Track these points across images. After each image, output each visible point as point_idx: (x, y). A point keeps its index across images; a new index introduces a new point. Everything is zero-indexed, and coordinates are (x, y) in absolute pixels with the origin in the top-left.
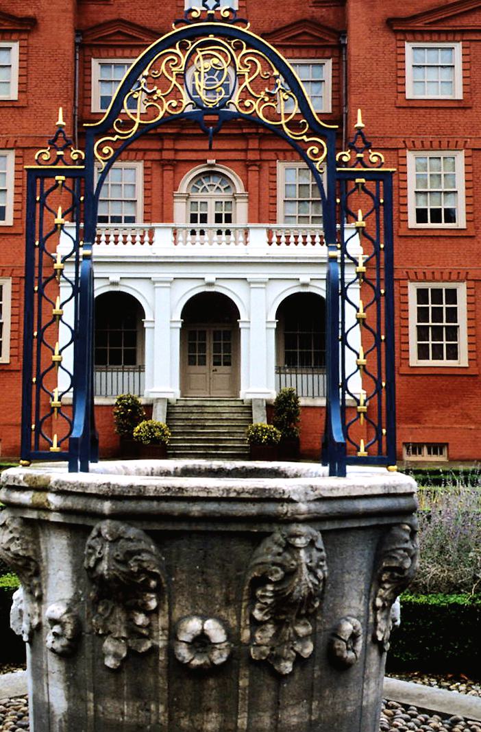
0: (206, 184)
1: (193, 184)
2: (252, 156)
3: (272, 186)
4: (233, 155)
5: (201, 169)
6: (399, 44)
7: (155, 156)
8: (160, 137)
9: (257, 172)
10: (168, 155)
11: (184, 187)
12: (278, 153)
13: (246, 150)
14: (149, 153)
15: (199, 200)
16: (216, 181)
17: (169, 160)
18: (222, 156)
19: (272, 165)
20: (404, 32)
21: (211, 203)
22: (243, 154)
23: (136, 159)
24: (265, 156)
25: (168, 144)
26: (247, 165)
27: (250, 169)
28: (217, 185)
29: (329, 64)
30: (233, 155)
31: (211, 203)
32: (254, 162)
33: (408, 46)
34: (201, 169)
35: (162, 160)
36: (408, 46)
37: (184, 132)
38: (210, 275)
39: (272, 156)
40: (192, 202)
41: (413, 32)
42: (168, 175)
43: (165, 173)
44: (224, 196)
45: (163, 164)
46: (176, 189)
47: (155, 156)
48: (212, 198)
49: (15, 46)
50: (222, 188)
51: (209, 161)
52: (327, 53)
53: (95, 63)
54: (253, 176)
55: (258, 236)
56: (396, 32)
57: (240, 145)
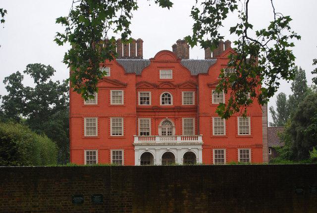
4: (172, 116)
5: (164, 120)
8: (155, 112)
10: (156, 117)
11: (160, 125)
21: (167, 128)
25: (157, 114)
26: (175, 119)
29: (194, 93)
30: (172, 116)
31: (167, 128)
32: (177, 118)
34: (164, 120)
39: (181, 116)
44: (170, 126)
48: (167, 127)
49: (123, 91)
55: (179, 139)
57: (173, 114)
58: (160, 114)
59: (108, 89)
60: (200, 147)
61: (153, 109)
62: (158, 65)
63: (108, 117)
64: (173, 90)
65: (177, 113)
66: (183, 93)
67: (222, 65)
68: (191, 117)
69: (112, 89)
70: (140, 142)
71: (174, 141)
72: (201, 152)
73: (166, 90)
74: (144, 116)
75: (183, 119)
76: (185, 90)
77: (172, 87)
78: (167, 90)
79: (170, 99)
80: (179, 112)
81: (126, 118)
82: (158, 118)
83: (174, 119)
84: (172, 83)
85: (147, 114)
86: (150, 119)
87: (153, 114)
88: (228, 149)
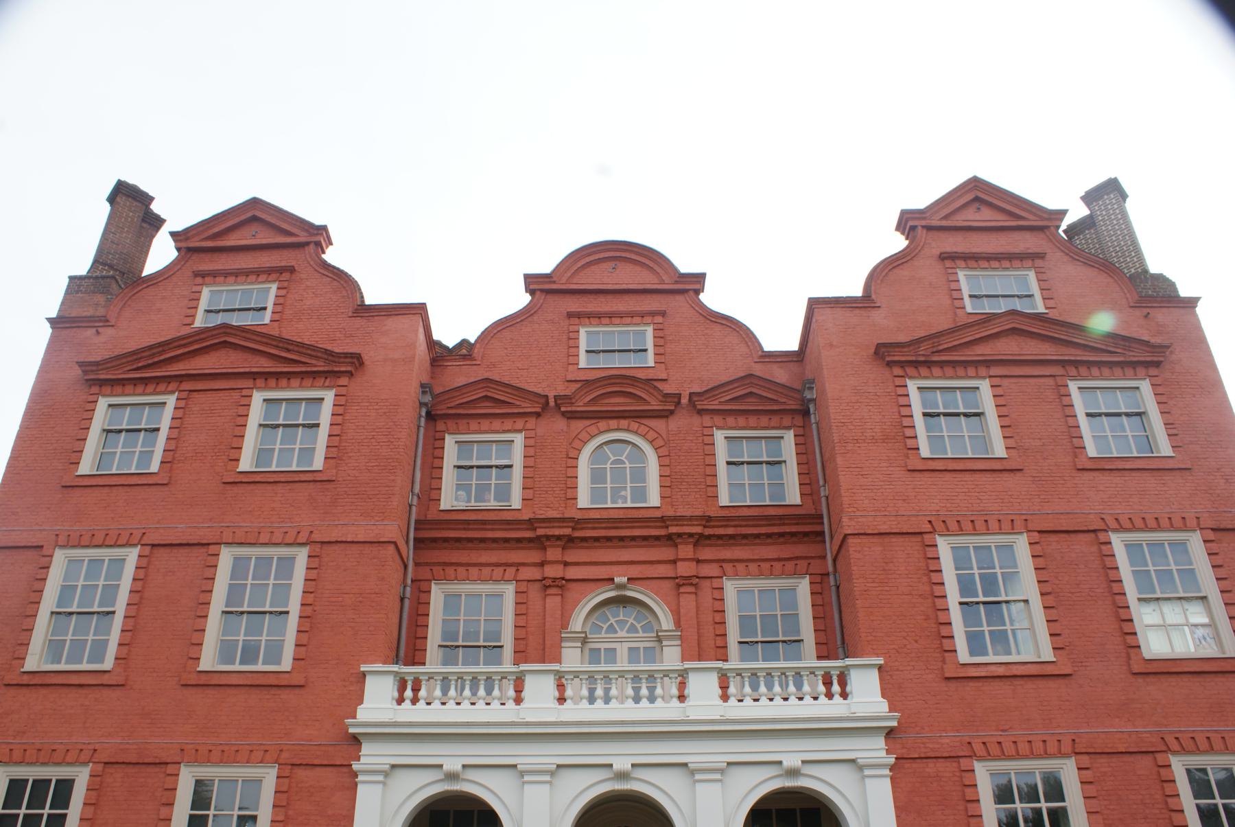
0: (612, 621)
1: (593, 619)
2: (684, 569)
3: (717, 605)
6: (898, 381)
7: (533, 573)
9: (694, 596)
10: (552, 571)
11: (577, 623)
12: (724, 565)
13: (674, 562)
14: (522, 569)
15: (603, 646)
16: (628, 616)
17: (554, 579)
18: (635, 571)
19: (716, 583)
20: (902, 364)
22: (669, 567)
23: (503, 580)
24: (706, 570)
25: (553, 553)
27: (682, 590)
28: (631, 620)
29: (789, 437)
33: (912, 386)
35: (544, 579)
36: (912, 386)
37: (577, 534)
38: (622, 757)
40: (591, 650)
41: (916, 364)
42: (553, 602)
43: (549, 600)
44: (643, 640)
45: (547, 585)
46: (565, 625)
47: (533, 573)
50: (638, 626)
51: (617, 580)
52: (787, 420)
53: (450, 441)
54: (688, 602)
56: (890, 364)
57: (666, 553)
58: (573, 555)
59: (249, 383)
60: (875, 750)
61: (531, 523)
62: (574, 304)
63: (207, 548)
64: (654, 423)
65: (686, 550)
66: (719, 436)
67: (943, 257)
68: (783, 574)
69: (266, 388)
70: (410, 713)
71: (665, 710)
72: (880, 795)
73: (613, 423)
74: (461, 570)
75: (731, 588)
76: (731, 420)
77: (655, 405)
78: (624, 423)
79: (639, 475)
80: (699, 540)
81: (320, 548)
82: (560, 585)
83: (667, 585)
84: (659, 385)
85: (485, 557)
86: (509, 591)
87: (534, 556)
88: (1087, 755)
